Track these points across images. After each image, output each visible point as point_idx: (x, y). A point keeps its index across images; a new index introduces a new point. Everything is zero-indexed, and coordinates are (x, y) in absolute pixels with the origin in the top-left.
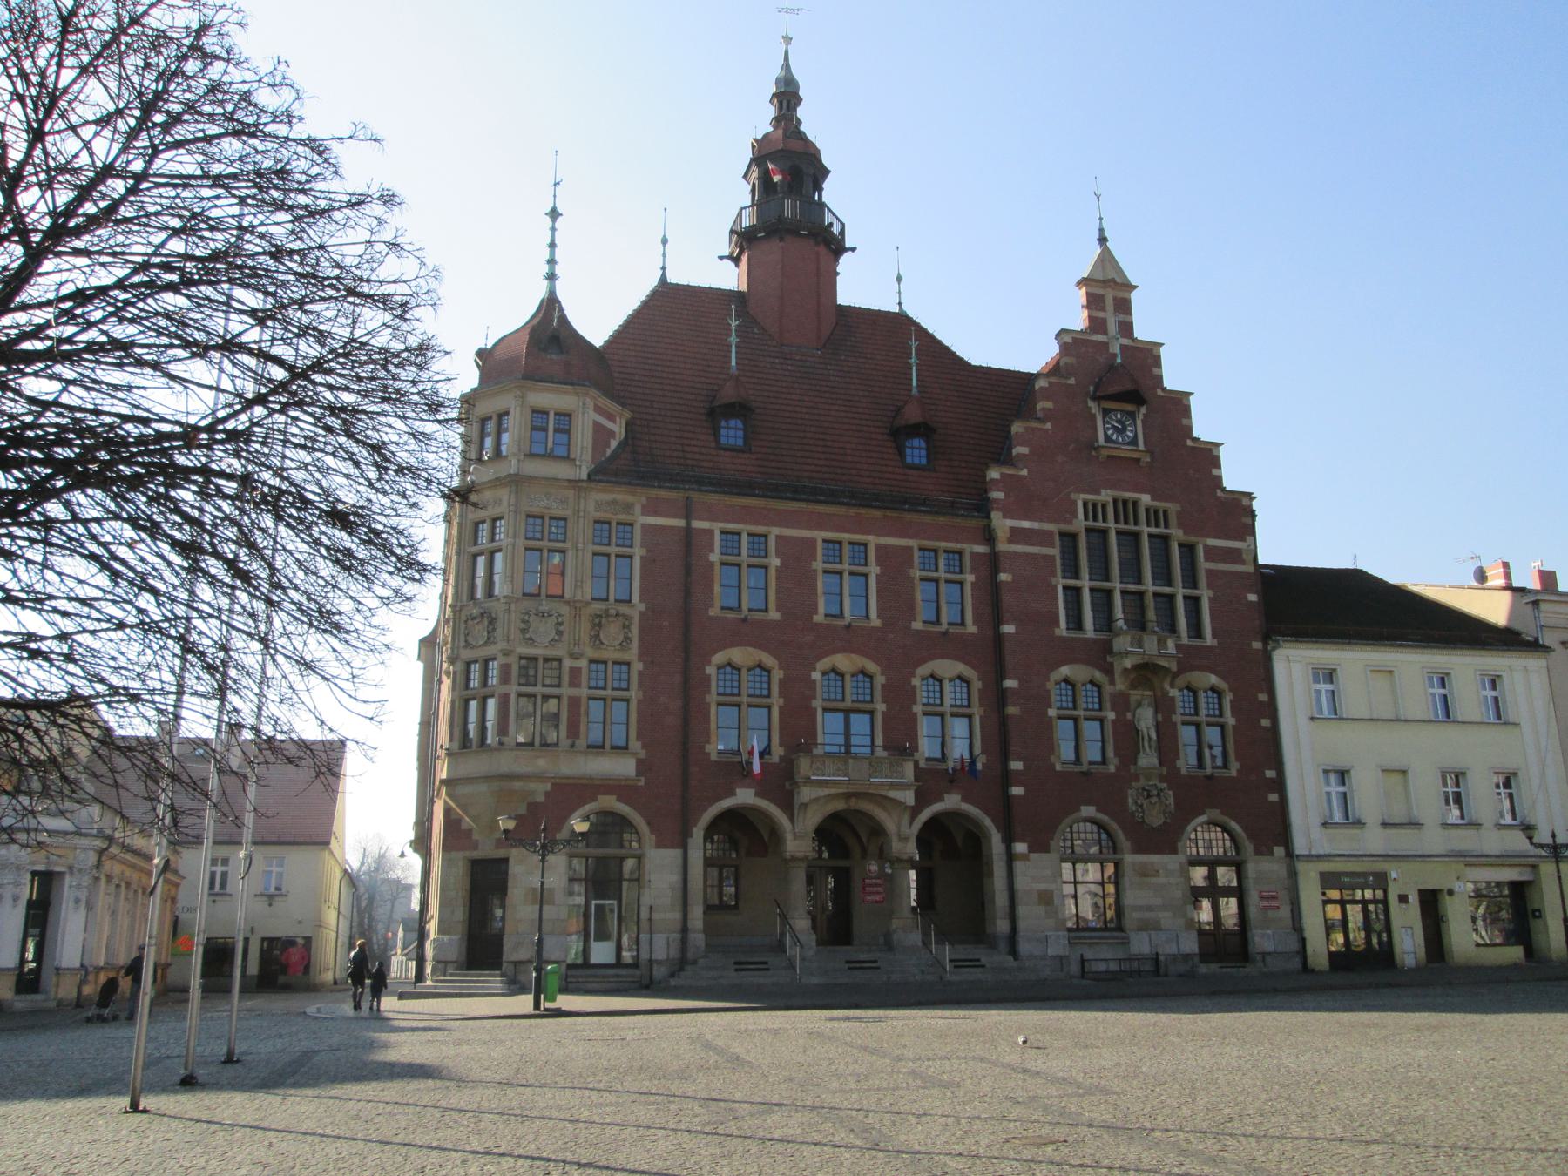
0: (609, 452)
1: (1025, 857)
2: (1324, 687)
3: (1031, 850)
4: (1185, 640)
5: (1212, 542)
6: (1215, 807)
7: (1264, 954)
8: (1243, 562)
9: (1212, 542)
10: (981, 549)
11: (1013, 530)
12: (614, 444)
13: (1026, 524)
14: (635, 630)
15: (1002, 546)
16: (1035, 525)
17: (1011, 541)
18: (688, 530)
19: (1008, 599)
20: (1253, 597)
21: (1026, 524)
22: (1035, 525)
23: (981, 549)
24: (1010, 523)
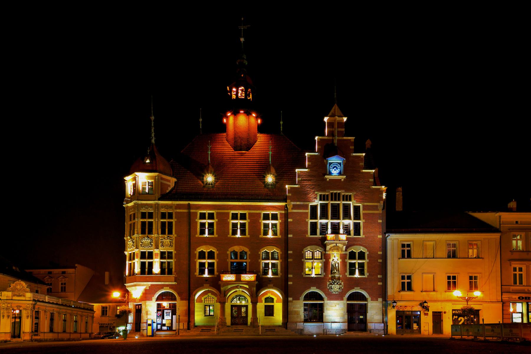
0: (168, 191)
1: (291, 301)
2: (406, 249)
3: (293, 299)
4: (352, 235)
5: (366, 204)
6: (357, 286)
7: (370, 331)
8: (378, 210)
9: (366, 204)
10: (283, 212)
11: (293, 205)
12: (170, 189)
13: (298, 203)
14: (174, 242)
15: (290, 211)
16: (302, 203)
17: (292, 209)
18: (189, 213)
19: (290, 227)
20: (380, 221)
21: (298, 203)
22: (302, 203)
23: (283, 212)
24: (293, 203)
